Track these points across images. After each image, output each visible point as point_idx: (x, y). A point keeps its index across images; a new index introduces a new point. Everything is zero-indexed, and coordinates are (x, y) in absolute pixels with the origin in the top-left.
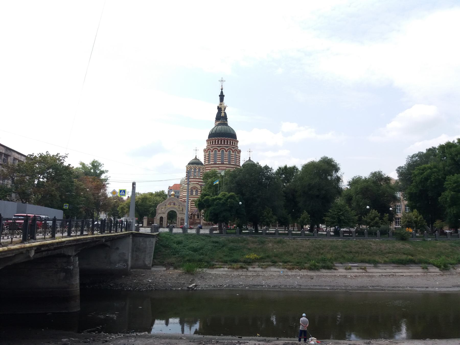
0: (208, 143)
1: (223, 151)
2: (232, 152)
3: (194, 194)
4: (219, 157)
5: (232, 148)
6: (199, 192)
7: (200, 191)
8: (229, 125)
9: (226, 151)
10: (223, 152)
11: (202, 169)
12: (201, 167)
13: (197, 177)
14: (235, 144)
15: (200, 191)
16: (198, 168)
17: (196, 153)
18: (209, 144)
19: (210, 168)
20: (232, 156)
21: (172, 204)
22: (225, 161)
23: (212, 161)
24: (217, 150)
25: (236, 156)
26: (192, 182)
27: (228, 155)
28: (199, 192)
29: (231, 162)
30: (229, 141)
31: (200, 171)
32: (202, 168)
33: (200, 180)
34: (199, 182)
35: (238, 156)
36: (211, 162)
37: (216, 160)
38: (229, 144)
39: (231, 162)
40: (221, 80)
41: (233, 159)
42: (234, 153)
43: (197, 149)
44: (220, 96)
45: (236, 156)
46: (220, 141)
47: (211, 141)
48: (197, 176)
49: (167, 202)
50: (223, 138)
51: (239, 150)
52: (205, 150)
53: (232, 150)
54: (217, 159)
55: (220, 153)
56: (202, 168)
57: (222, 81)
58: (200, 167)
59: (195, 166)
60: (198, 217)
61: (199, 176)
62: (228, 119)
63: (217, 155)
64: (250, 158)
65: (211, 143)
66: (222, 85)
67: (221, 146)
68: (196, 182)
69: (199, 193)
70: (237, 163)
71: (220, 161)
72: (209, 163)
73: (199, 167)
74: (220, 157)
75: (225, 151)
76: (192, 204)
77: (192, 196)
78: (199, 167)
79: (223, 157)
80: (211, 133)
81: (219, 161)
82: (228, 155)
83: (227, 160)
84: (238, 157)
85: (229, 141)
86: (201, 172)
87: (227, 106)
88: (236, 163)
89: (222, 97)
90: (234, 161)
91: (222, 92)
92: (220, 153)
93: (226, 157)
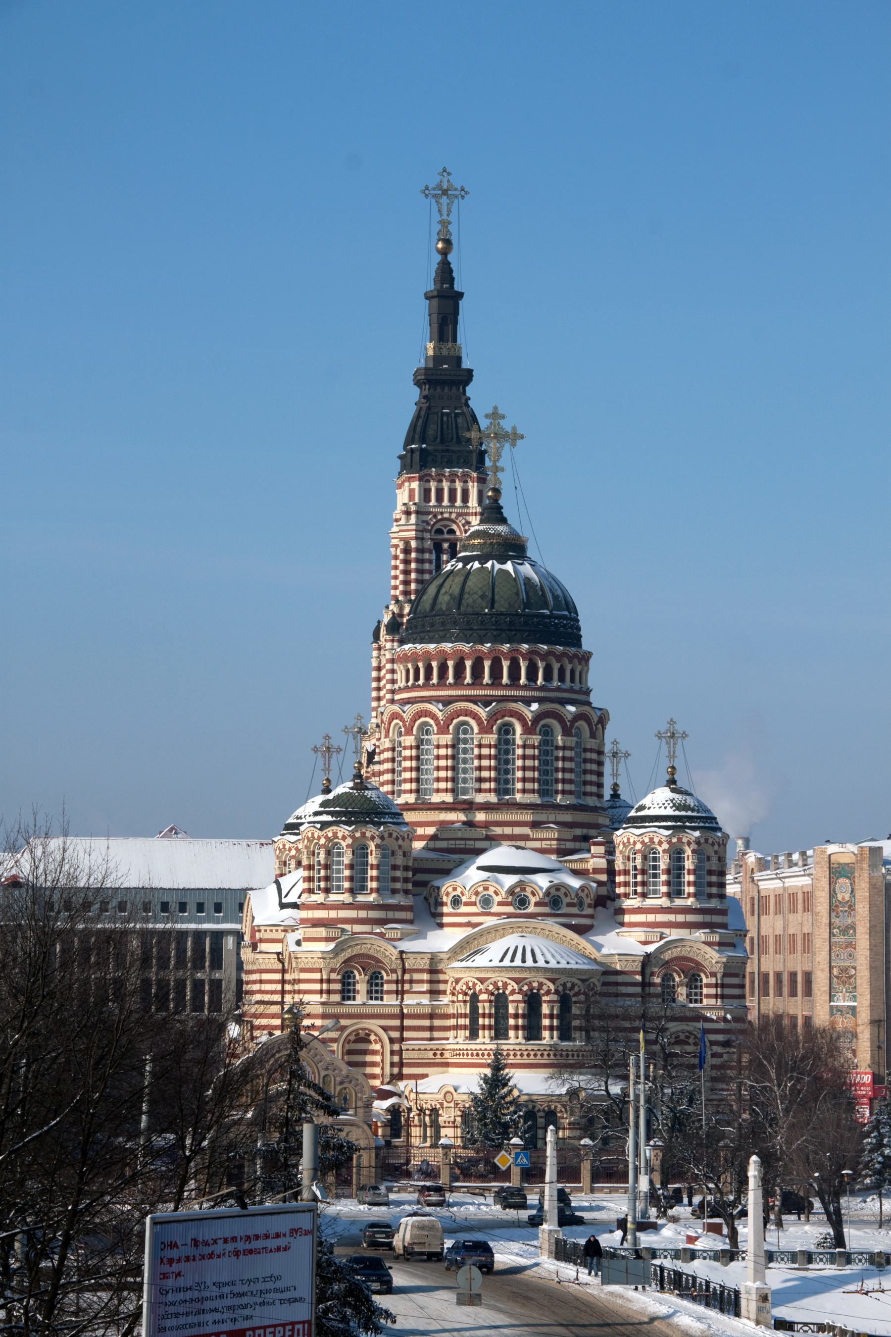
6: (393, 987)
7: (397, 982)
10: (507, 732)
11: (400, 847)
18: (417, 678)
23: (446, 790)
24: (473, 723)
25: (585, 750)
31: (392, 861)
40: (439, 187)
44: (428, 297)
45: (585, 750)
46: (487, 664)
47: (434, 664)
57: (445, 192)
58: (390, 835)
65: (428, 676)
66: (445, 224)
76: (350, 1052)
81: (490, 791)
84: (594, 756)
87: (519, 431)
91: (445, 273)
92: (492, 738)
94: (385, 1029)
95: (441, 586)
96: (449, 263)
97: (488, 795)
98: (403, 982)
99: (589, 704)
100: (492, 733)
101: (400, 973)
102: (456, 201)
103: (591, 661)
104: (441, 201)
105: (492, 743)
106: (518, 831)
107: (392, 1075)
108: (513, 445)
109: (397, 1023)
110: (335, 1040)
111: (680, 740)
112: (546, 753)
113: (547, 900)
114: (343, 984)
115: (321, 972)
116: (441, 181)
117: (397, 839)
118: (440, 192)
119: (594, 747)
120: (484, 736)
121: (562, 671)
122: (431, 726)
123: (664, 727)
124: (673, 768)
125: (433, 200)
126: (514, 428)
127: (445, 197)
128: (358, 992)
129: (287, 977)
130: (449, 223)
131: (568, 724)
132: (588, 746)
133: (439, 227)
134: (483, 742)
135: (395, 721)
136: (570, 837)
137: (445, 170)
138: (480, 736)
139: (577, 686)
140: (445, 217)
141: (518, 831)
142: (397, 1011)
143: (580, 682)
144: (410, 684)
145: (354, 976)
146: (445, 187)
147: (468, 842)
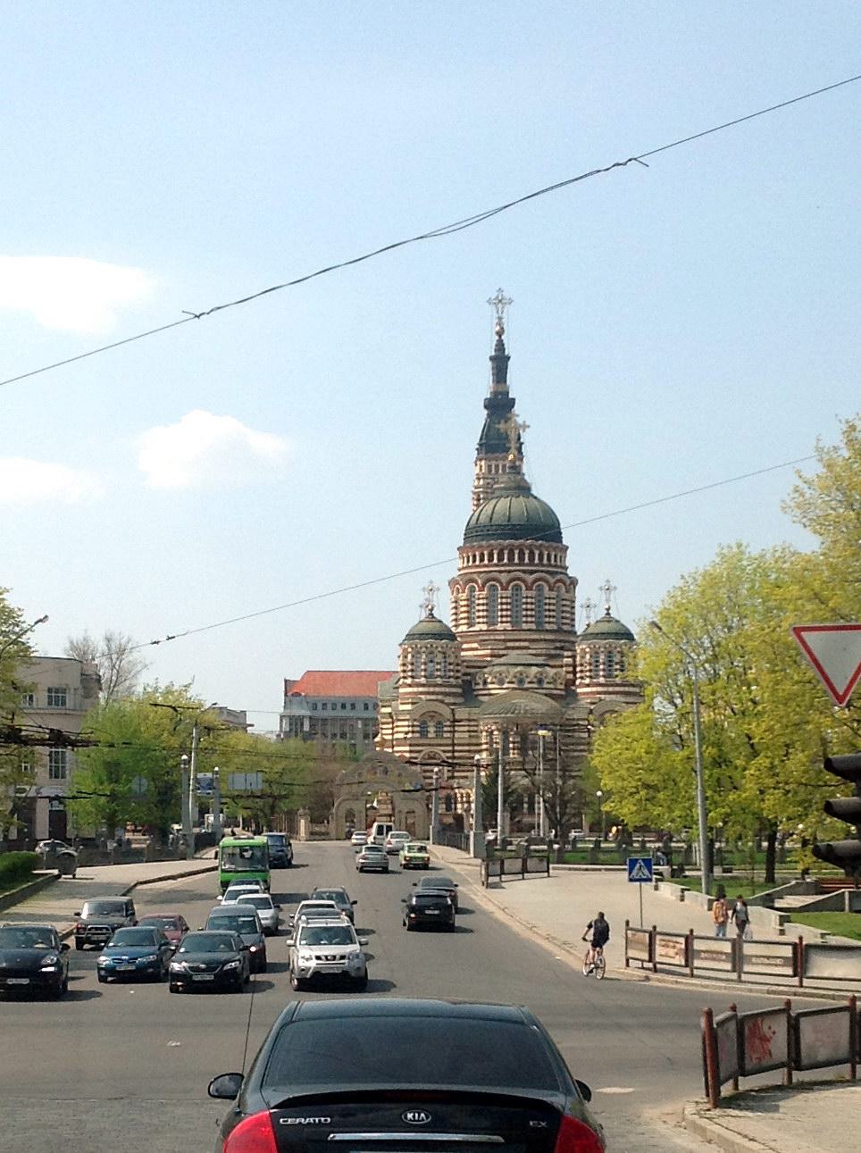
0: (466, 559)
1: (517, 588)
5: (548, 576)
6: (449, 729)
8: (534, 492)
10: (517, 590)
11: (453, 653)
13: (439, 679)
15: (448, 723)
18: (468, 561)
19: (475, 645)
20: (547, 601)
23: (483, 623)
24: (498, 584)
27: (533, 600)
28: (445, 729)
29: (546, 623)
30: (537, 553)
31: (448, 660)
33: (447, 690)
34: (446, 694)
36: (479, 623)
38: (537, 561)
39: (546, 623)
41: (552, 613)
44: (492, 359)
48: (438, 676)
51: (570, 578)
52: (453, 583)
53: (547, 582)
55: (509, 593)
57: (500, 301)
66: (500, 318)
67: (509, 572)
69: (446, 732)
72: (471, 626)
75: (524, 588)
77: (427, 741)
80: (477, 523)
82: (533, 600)
83: (532, 616)
84: (568, 603)
85: (537, 553)
87: (527, 423)
88: (563, 624)
89: (500, 362)
91: (500, 346)
92: (509, 593)
93: (529, 606)
94: (444, 751)
95: (482, 510)
96: (502, 341)
97: (505, 624)
98: (454, 726)
99: (567, 575)
100: (506, 589)
103: (568, 552)
106: (522, 644)
109: (450, 748)
112: (539, 601)
113: (535, 680)
126: (524, 422)
129: (395, 725)
132: (564, 598)
133: (497, 320)
134: (504, 595)
136: (552, 647)
139: (559, 564)
141: (522, 644)
142: (450, 742)
144: (465, 564)
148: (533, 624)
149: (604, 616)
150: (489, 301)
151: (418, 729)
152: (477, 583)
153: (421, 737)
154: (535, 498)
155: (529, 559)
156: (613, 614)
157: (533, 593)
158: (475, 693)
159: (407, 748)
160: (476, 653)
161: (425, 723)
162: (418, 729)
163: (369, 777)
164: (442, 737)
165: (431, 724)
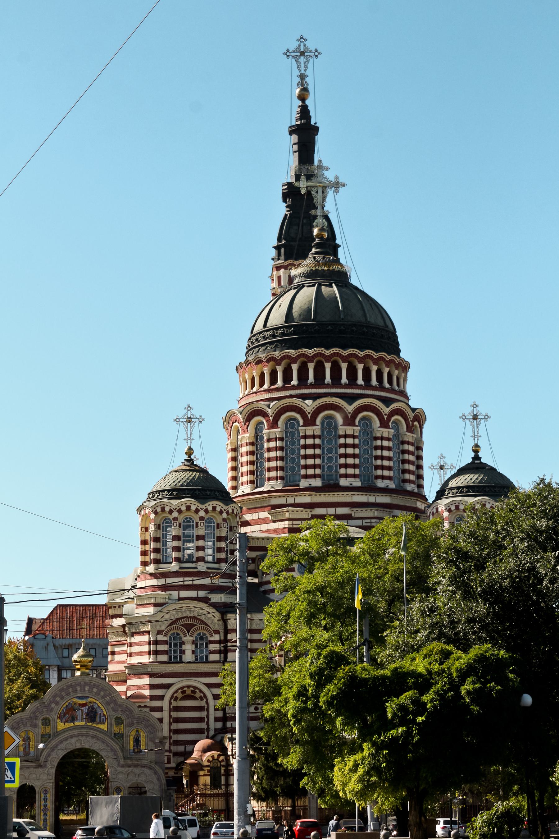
2: (381, 427)
3: (188, 656)
4: (310, 452)
7: (219, 642)
9: (349, 421)
11: (225, 520)
12: (218, 509)
14: (390, 381)
15: (216, 637)
16: (202, 513)
17: (189, 439)
18: (253, 386)
20: (379, 443)
21: (79, 713)
22: (342, 476)
23: (276, 478)
24: (298, 416)
25: (403, 443)
26: (175, 594)
27: (357, 441)
29: (377, 477)
31: (217, 533)
32: (225, 515)
34: (213, 589)
35: (412, 444)
37: (293, 469)
38: (360, 381)
39: (377, 477)
40: (298, 50)
41: (386, 463)
42: (387, 426)
43: (196, 413)
45: (403, 443)
46: (311, 367)
48: (199, 559)
49: (51, 702)
50: (328, 352)
51: (414, 410)
54: (303, 462)
55: (316, 430)
56: (225, 515)
57: (302, 54)
58: (214, 509)
59: (188, 508)
60: (215, 783)
61: (210, 559)
62: (340, 250)
63: (302, 442)
64: (476, 449)
66: (303, 77)
68: (193, 594)
69: (214, 652)
70: (409, 481)
71: (319, 476)
72: (257, 487)
73: (206, 511)
74: (318, 451)
76: (177, 709)
78: (206, 511)
79: (330, 451)
80: (265, 326)
81: (314, 476)
83: (354, 466)
84: (411, 448)
86: (220, 539)
87: (341, 180)
90: (391, 473)
96: (307, 106)
100: (314, 424)
101: (222, 634)
102: (311, 60)
104: (299, 60)
105: (316, 434)
107: (216, 730)
108: (337, 192)
110: (161, 698)
111: (483, 421)
114: (170, 646)
115: (149, 635)
116: (299, 46)
117: (221, 512)
118: (299, 54)
119: (410, 440)
120: (307, 427)
121: (379, 373)
122: (263, 423)
123: (468, 411)
124: (477, 446)
125: (293, 60)
126: (337, 178)
127: (302, 57)
128: (184, 652)
130: (307, 76)
131: (386, 417)
132: (406, 439)
133: (299, 79)
135: (234, 424)
137: (302, 38)
138: (304, 428)
139: (397, 388)
140: (303, 72)
143: (398, 385)
144: (246, 393)
145: (180, 638)
146: (302, 50)
147: (295, 522)
148: (358, 480)
149: (470, 461)
150: (287, 54)
151: (164, 647)
152: (264, 414)
153: (169, 662)
154: (356, 288)
155: (347, 378)
156: (486, 458)
157: (356, 430)
158: (263, 589)
159: (146, 681)
160: (264, 527)
161: (176, 636)
162: (164, 647)
163: (61, 726)
164: (207, 661)
165: (188, 638)
